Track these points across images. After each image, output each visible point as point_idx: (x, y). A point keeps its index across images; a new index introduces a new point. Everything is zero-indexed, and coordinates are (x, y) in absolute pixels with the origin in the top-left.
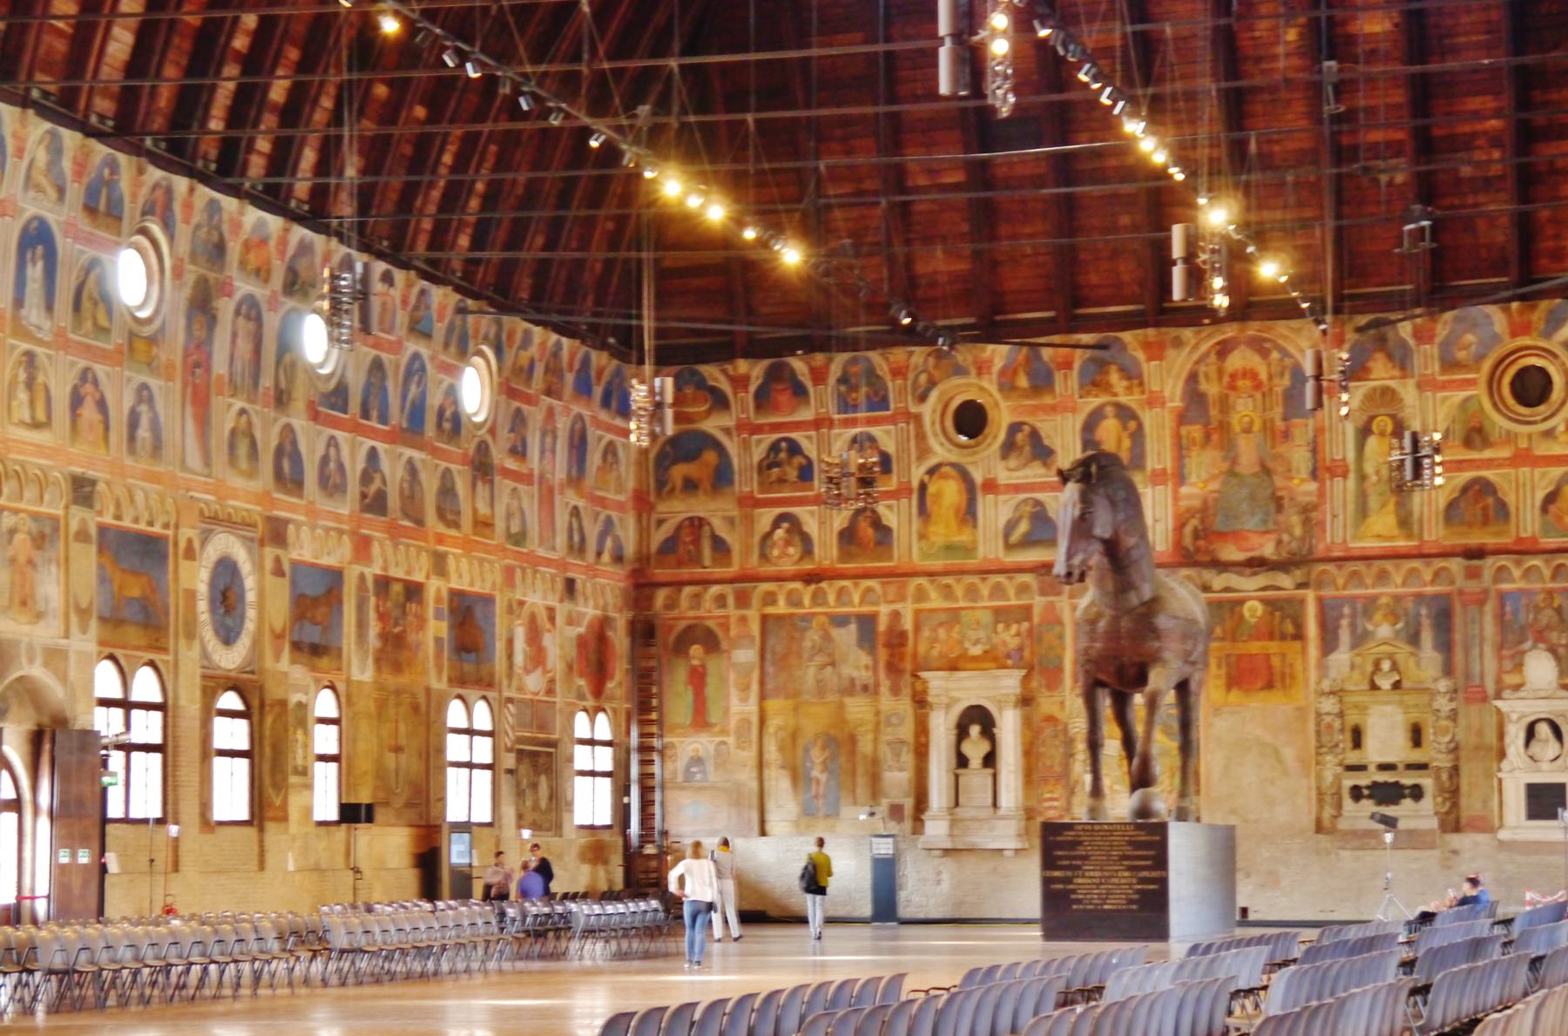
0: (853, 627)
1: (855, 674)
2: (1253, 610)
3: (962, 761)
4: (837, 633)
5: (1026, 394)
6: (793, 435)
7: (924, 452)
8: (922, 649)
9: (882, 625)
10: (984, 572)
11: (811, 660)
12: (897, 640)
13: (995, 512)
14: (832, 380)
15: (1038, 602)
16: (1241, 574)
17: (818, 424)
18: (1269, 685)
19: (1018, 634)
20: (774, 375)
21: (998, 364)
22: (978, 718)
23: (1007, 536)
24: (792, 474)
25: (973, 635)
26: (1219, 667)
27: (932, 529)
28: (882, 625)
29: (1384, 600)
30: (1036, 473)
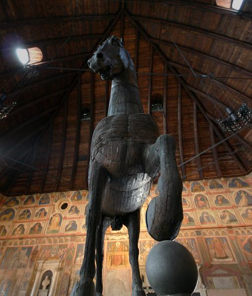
0: (26, 250)
1: (23, 262)
2: (118, 244)
3: (41, 287)
4: (22, 251)
5: (76, 201)
6: (29, 209)
7: (54, 211)
8: (40, 255)
9: (33, 250)
10: (59, 237)
11: (14, 259)
12: (36, 252)
13: (65, 223)
14: (40, 199)
15: (69, 243)
16: (116, 236)
17: (34, 207)
18: (122, 264)
19: (64, 251)
20: (29, 198)
21: (72, 195)
22: (49, 274)
23: (66, 228)
24: (26, 216)
25: (53, 251)
26: (109, 259)
27: (51, 227)
28: (33, 250)
29: (147, 242)
30: (75, 215)
